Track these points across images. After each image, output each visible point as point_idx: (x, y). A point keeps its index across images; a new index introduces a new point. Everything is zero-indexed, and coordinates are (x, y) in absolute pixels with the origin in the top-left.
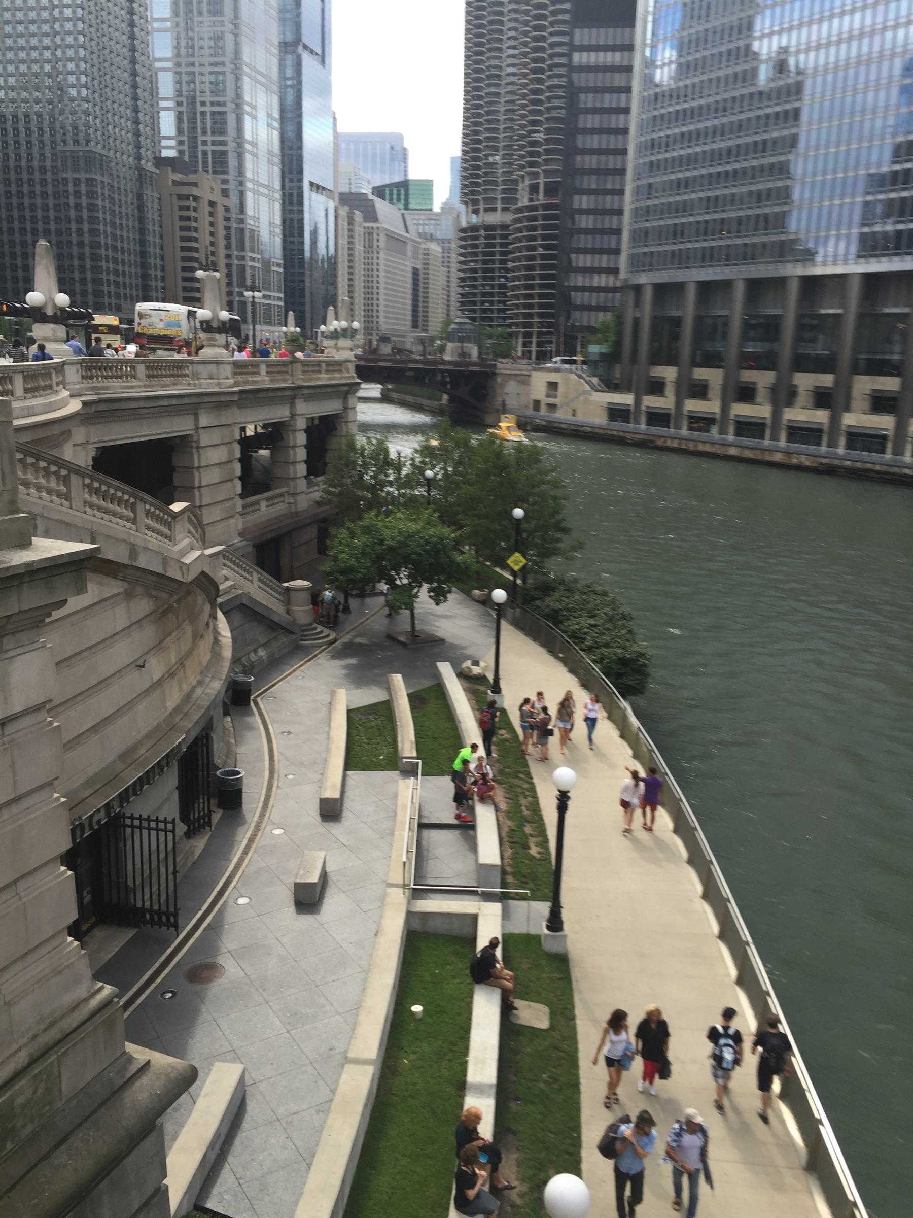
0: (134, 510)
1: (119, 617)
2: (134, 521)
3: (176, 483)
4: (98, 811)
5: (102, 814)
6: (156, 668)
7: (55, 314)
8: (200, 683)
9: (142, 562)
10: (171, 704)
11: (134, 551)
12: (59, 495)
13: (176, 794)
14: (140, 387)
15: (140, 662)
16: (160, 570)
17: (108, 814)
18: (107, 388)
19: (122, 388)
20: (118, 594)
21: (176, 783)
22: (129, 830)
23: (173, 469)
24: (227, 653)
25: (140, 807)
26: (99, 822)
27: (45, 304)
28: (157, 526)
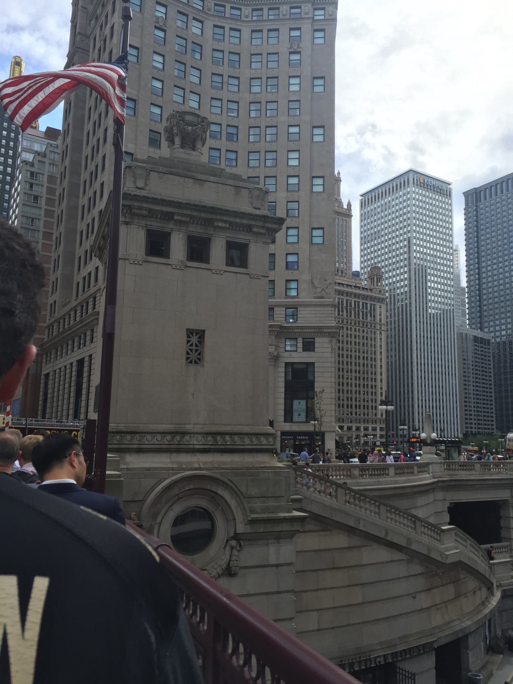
0: (415, 524)
1: (402, 570)
2: (415, 529)
3: (502, 525)
4: (380, 656)
5: (382, 659)
6: (424, 601)
7: (431, 442)
8: (458, 619)
9: (414, 547)
10: (434, 624)
11: (409, 541)
12: (375, 513)
13: (434, 671)
14: (476, 474)
15: (414, 596)
16: (425, 552)
17: (385, 661)
18: (455, 475)
19: (466, 475)
20: (403, 560)
21: (434, 665)
22: (398, 674)
23: (501, 518)
24: (486, 611)
25: (408, 666)
26: (380, 662)
27: (427, 438)
28: (460, 541)
